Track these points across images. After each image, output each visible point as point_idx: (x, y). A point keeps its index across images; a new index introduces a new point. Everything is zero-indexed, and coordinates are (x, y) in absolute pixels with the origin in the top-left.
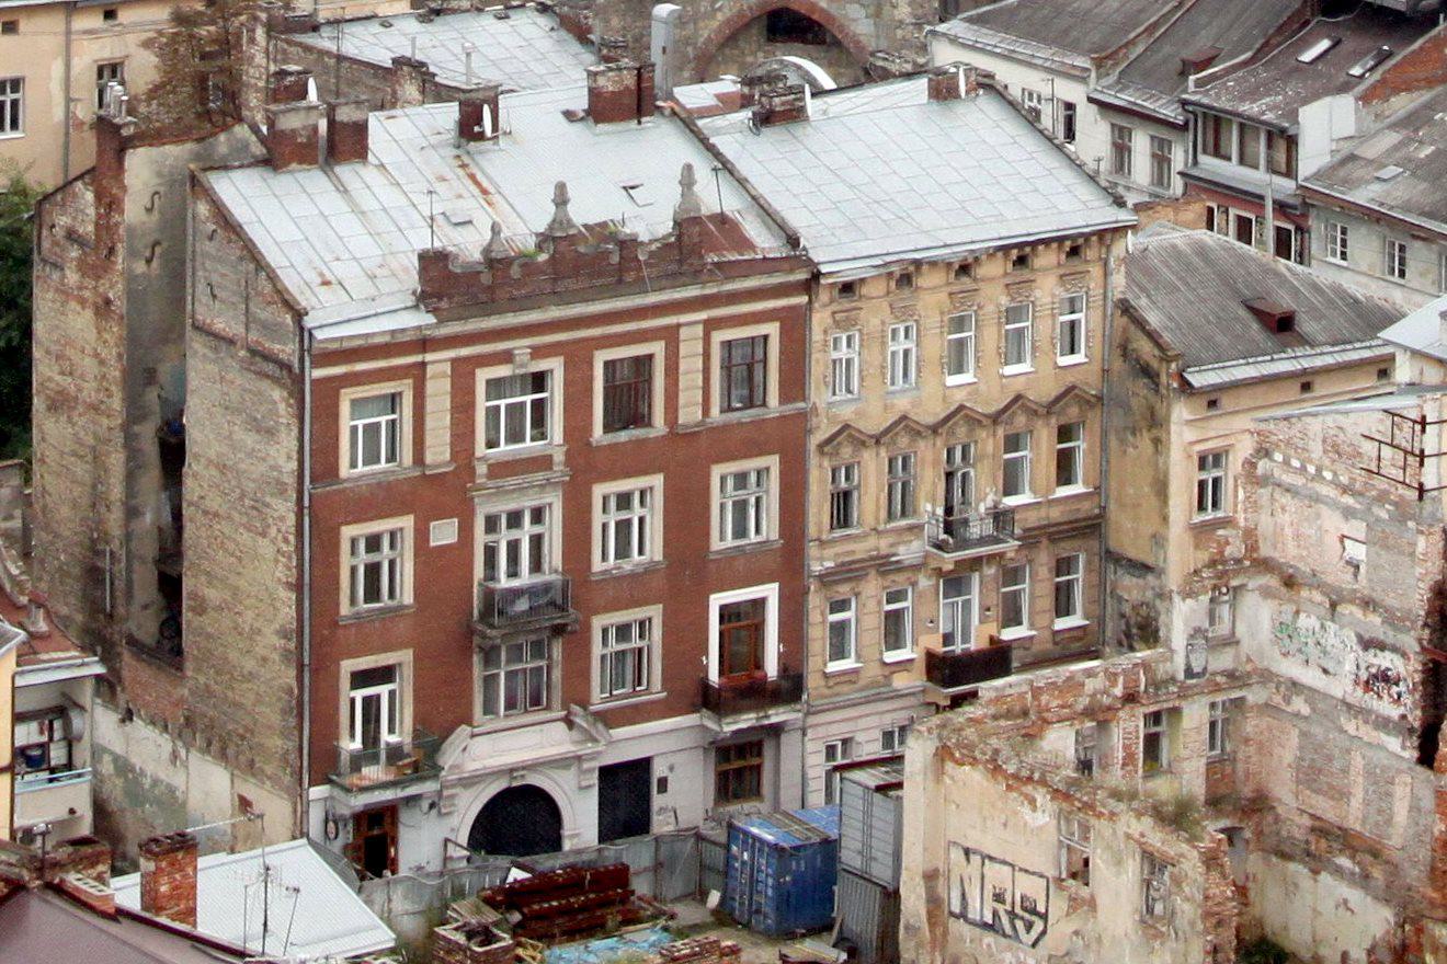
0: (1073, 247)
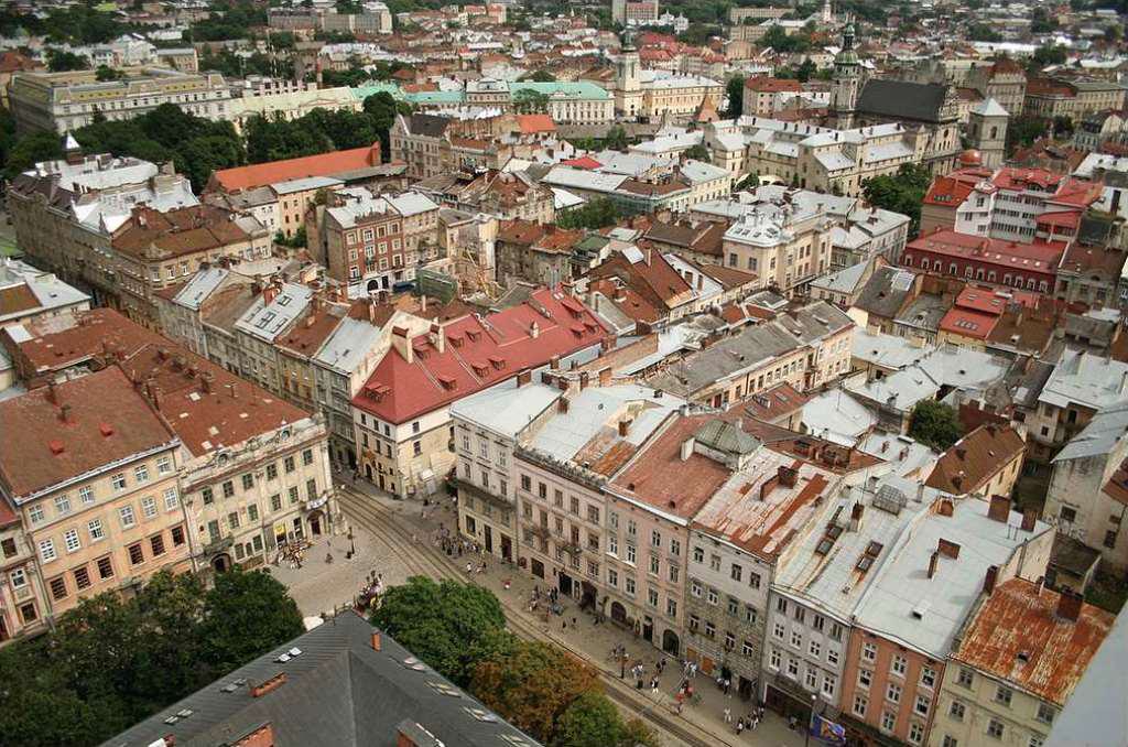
0: (433, 210)
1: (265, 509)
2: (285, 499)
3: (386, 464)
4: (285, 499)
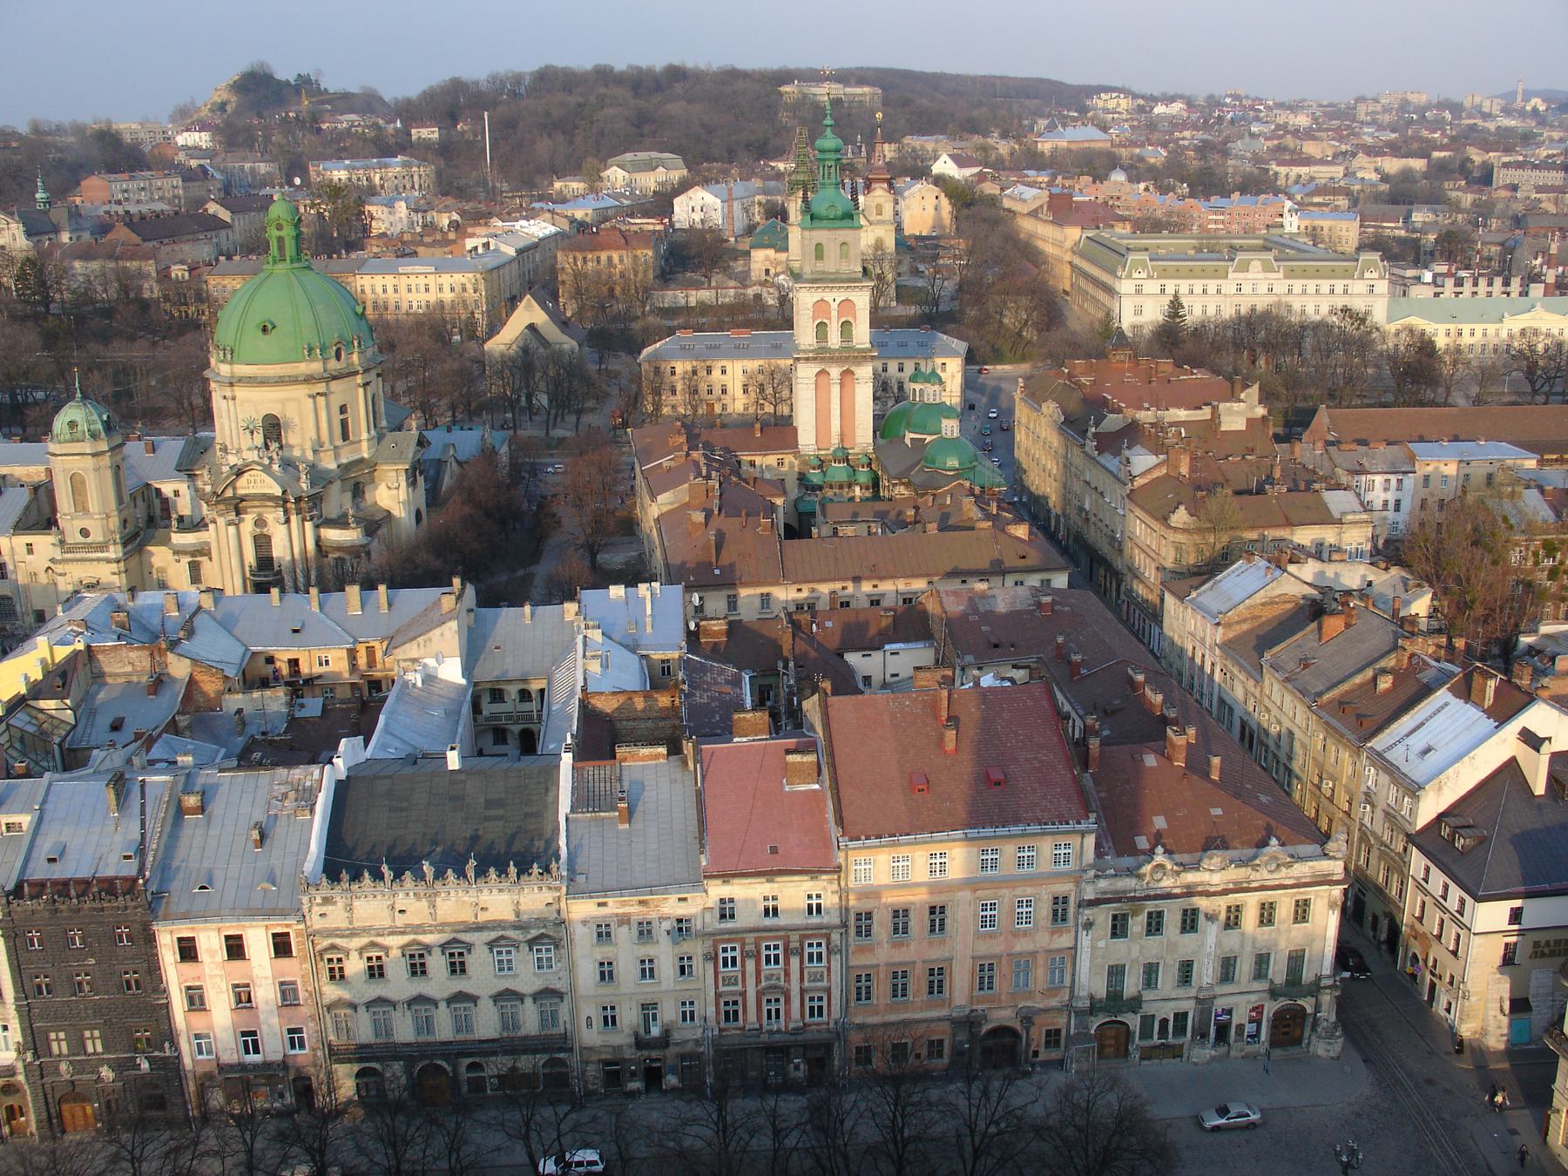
1: (1206, 973)
2: (1245, 968)
3: (1449, 967)
4: (1245, 968)
